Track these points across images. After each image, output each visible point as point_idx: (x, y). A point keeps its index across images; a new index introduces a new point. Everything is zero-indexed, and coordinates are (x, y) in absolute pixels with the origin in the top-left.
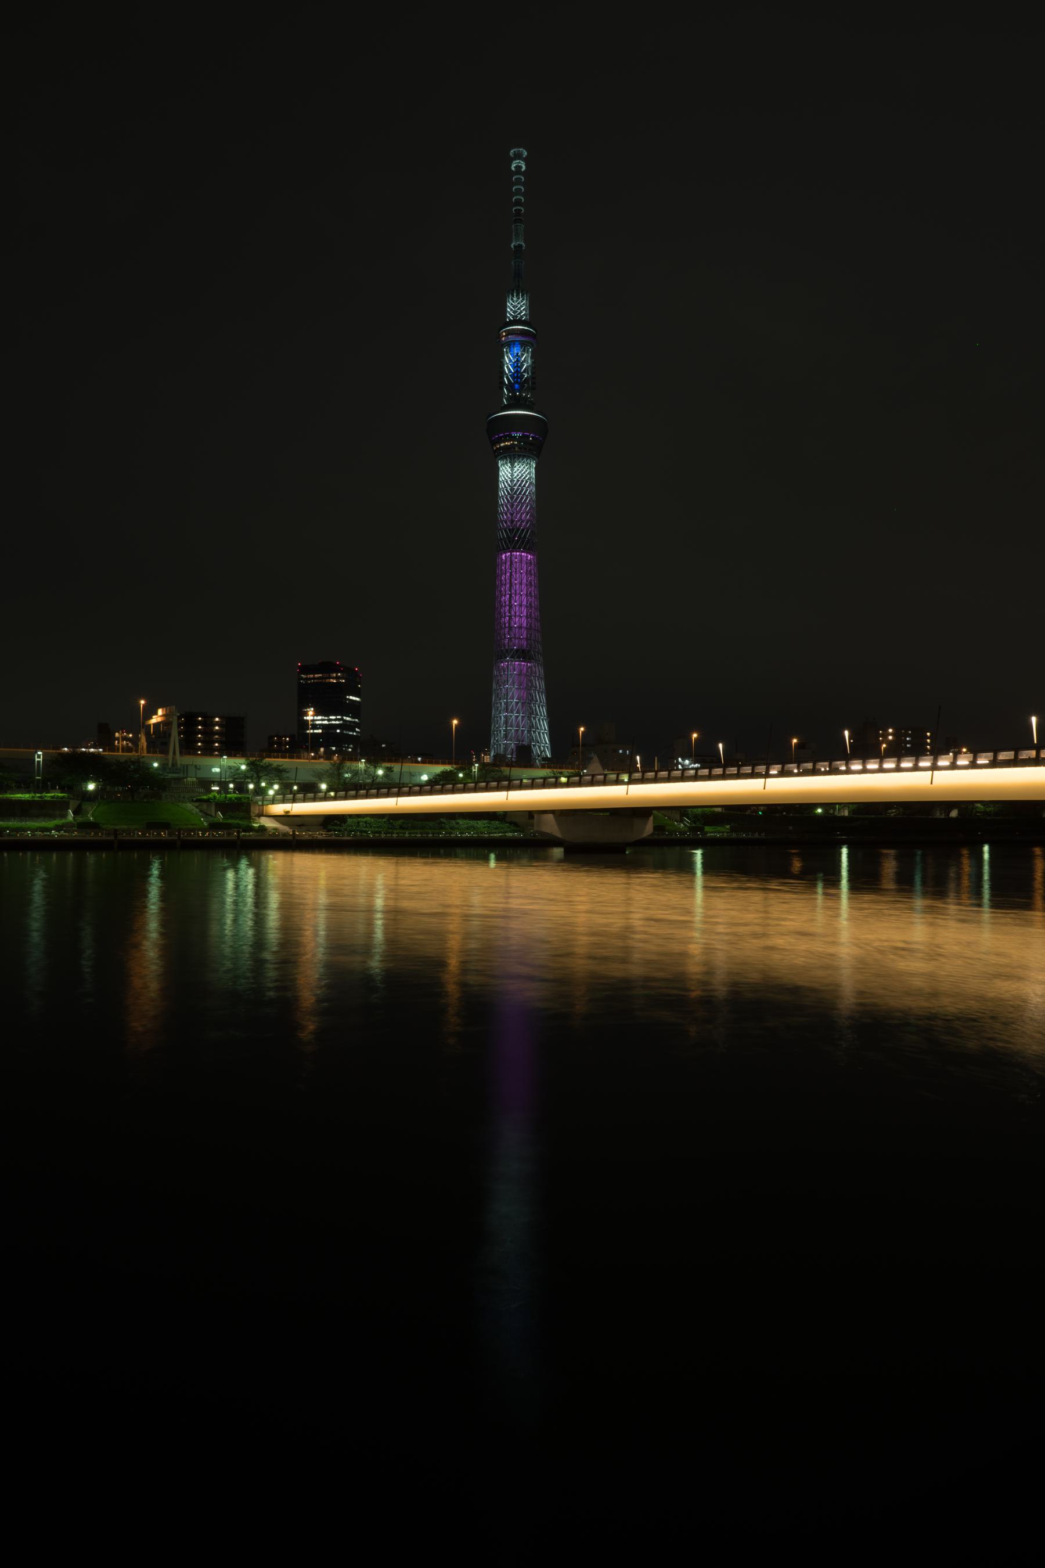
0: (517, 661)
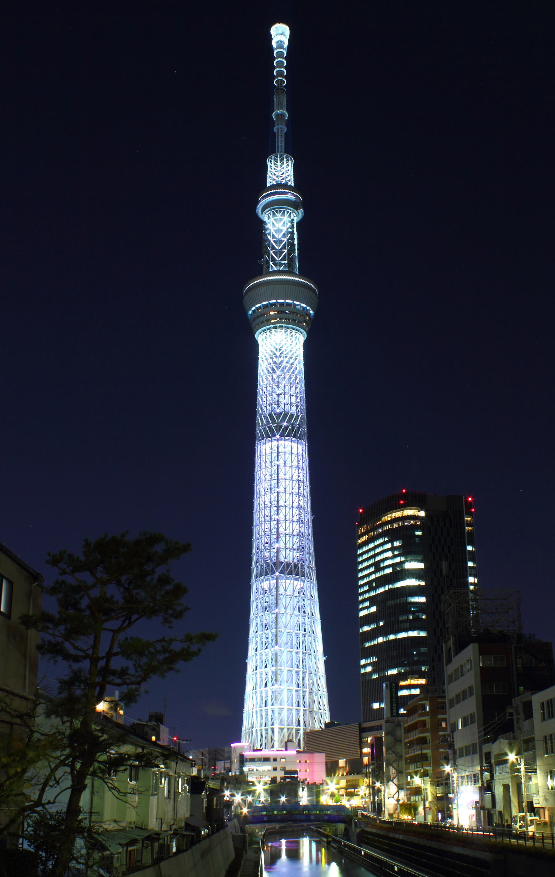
0: (287, 578)
